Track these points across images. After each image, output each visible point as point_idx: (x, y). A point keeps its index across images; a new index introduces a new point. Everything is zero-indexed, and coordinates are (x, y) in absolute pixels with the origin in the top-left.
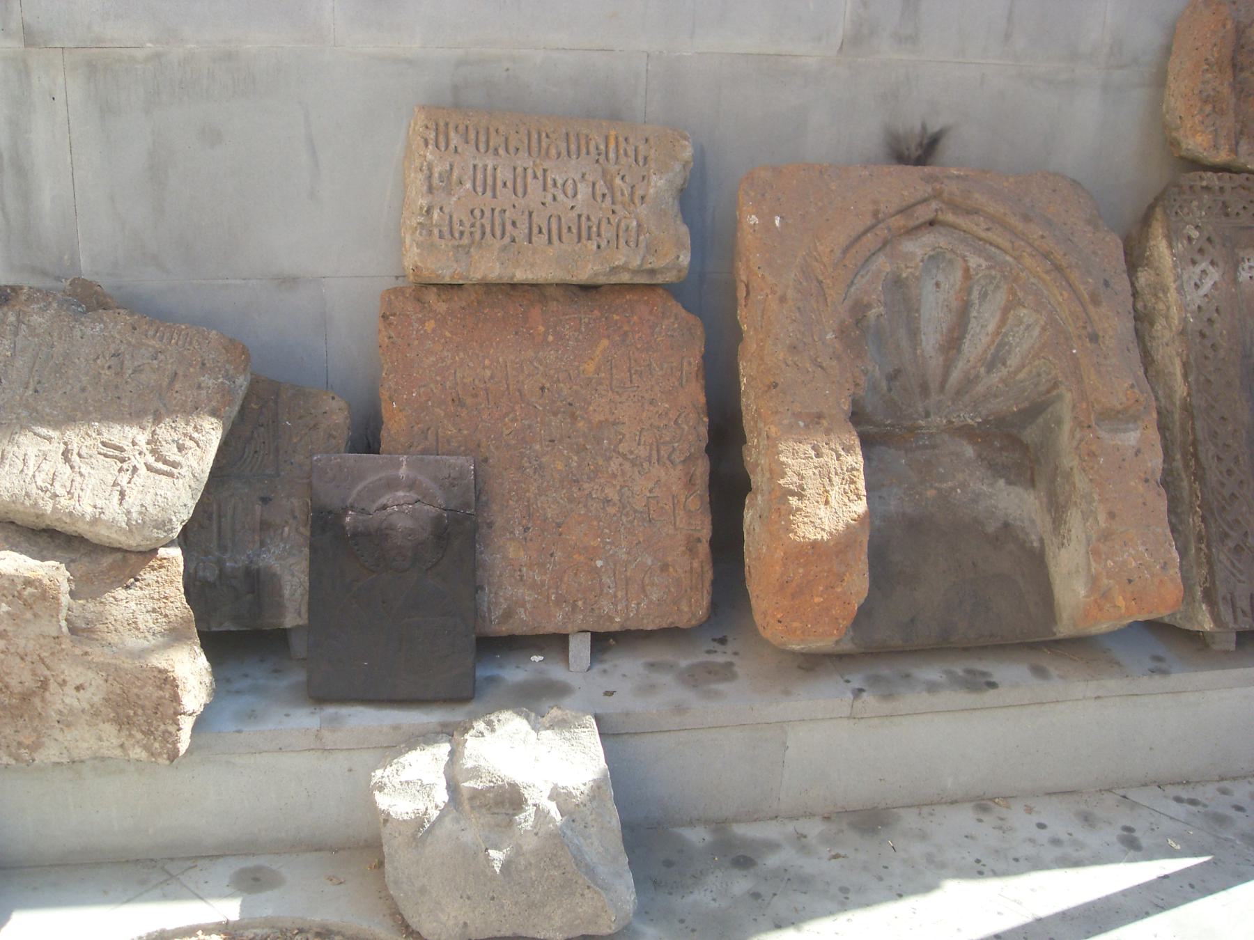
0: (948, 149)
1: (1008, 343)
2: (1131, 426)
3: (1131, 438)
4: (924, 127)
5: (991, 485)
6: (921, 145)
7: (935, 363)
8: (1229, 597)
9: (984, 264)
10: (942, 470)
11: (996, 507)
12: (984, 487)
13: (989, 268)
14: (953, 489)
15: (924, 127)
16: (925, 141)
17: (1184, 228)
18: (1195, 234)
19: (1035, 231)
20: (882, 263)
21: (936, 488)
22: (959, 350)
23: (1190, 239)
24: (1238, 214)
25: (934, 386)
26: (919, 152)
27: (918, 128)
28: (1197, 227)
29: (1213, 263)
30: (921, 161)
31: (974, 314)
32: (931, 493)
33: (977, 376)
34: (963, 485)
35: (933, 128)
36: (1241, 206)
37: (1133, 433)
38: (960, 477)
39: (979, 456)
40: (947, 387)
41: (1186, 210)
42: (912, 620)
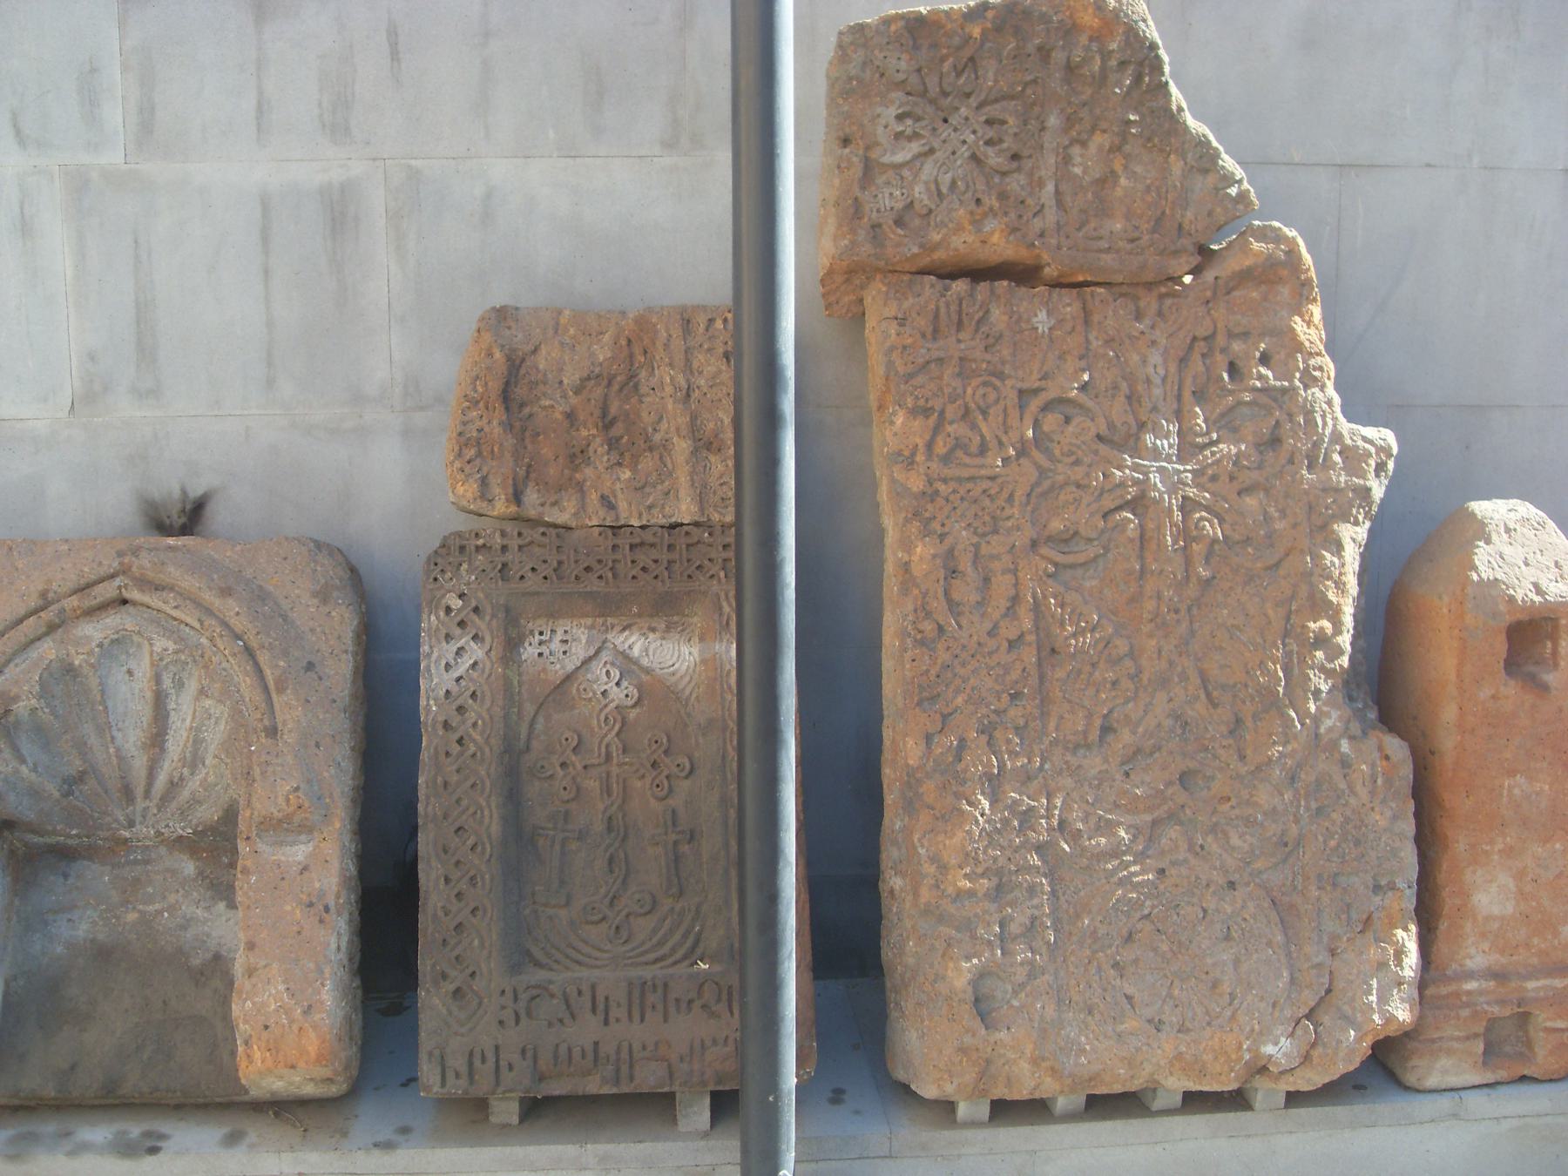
0: (218, 516)
1: (204, 740)
2: (303, 837)
3: (299, 852)
4: (184, 492)
5: (208, 908)
6: (183, 511)
7: (139, 763)
8: (437, 1052)
9: (171, 646)
10: (150, 890)
11: (208, 936)
12: (199, 912)
13: (176, 652)
14: (160, 912)
15: (184, 492)
16: (188, 507)
17: (444, 596)
18: (456, 603)
19: (231, 608)
20: (48, 650)
21: (140, 911)
22: (163, 750)
23: (448, 610)
24: (522, 577)
25: (139, 791)
26: (183, 520)
27: (177, 493)
28: (461, 596)
29: (475, 638)
30: (186, 530)
31: (172, 705)
32: (132, 917)
33: (181, 779)
34: (172, 909)
35: (196, 491)
36: (528, 567)
37: (303, 847)
38: (172, 898)
39: (200, 873)
40: (153, 791)
41: (449, 575)
42: (73, 1068)
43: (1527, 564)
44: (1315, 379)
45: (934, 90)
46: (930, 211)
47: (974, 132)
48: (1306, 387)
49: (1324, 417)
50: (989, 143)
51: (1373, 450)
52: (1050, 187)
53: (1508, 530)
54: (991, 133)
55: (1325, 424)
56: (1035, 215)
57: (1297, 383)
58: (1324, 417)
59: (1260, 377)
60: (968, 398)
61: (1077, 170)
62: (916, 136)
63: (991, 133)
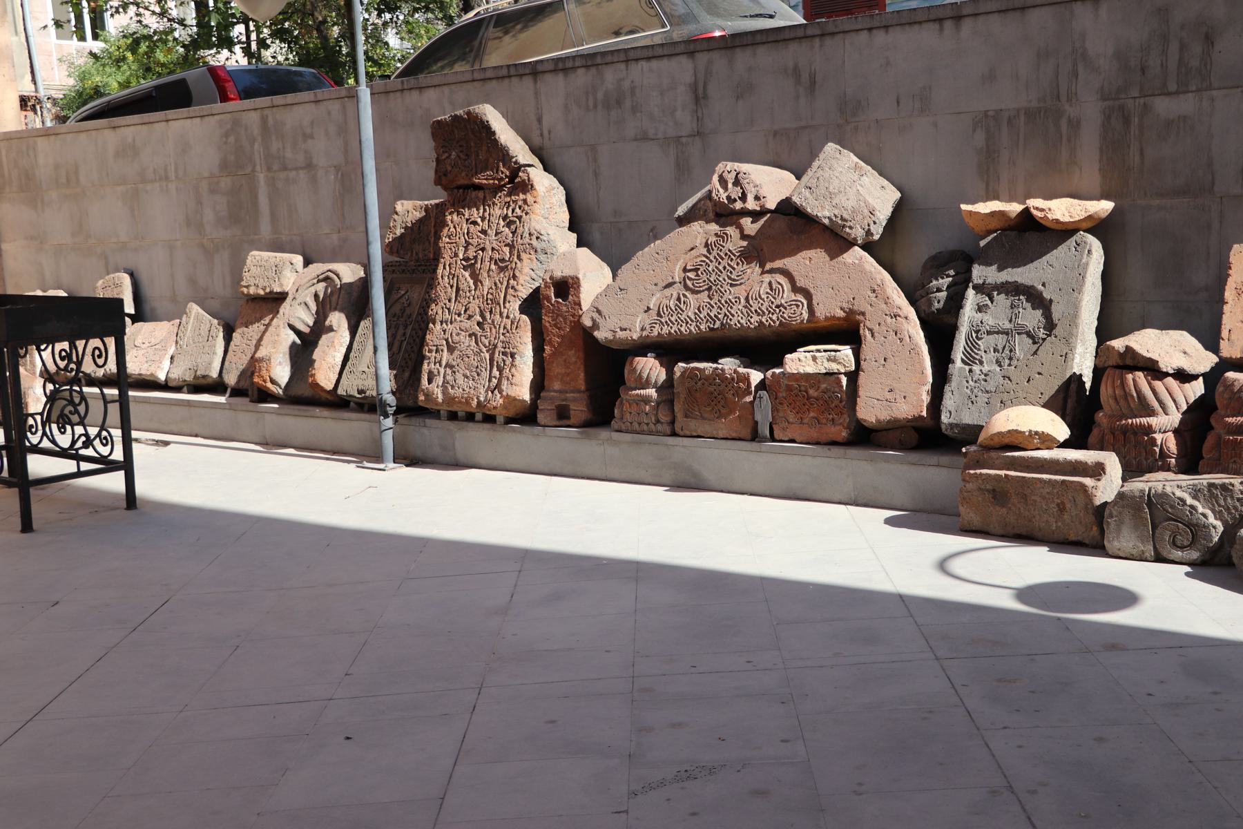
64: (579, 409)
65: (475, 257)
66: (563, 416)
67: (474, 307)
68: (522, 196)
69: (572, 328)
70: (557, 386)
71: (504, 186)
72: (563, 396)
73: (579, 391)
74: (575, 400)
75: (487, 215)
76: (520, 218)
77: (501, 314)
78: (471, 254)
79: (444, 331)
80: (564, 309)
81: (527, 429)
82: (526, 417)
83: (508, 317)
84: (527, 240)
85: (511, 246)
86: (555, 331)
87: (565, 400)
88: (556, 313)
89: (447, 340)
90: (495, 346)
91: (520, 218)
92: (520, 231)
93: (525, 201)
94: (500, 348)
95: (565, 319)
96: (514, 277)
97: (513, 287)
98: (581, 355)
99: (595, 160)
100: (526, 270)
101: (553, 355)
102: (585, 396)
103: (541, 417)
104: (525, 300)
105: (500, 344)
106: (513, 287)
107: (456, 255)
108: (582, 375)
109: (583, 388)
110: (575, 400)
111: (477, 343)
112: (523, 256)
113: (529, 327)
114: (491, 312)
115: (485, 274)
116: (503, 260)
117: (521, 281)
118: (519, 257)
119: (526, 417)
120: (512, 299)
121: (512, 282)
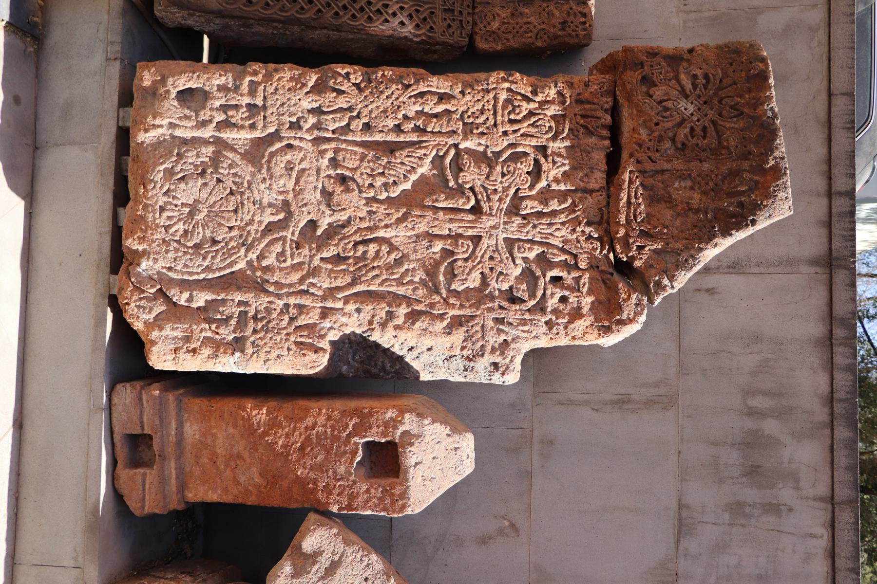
43: (434, 458)
44: (550, 329)
45: (722, 94)
46: (651, 96)
47: (698, 120)
48: (546, 323)
49: (528, 332)
50: (692, 129)
51: (507, 361)
52: (667, 166)
53: (456, 449)
54: (698, 130)
55: (524, 331)
56: (650, 158)
57: (549, 317)
58: (528, 332)
59: (552, 294)
60: (542, 117)
61: (677, 185)
62: (695, 86)
63: (698, 130)
64: (150, 495)
65: (460, 191)
66: (134, 449)
67: (353, 205)
68: (587, 302)
69: (301, 482)
70: (192, 431)
71: (612, 249)
72: (170, 449)
73: (182, 487)
74: (163, 480)
75: (554, 205)
76: (541, 308)
77: (331, 293)
78: (472, 176)
79: (295, 126)
80: (342, 470)
81: (101, 362)
82: (128, 354)
83: (325, 313)
84: (494, 339)
85: (480, 295)
86: (297, 440)
87: (163, 457)
88: (331, 445)
89: (275, 136)
90: (260, 288)
91: (541, 308)
92: (513, 314)
93: (576, 314)
94: (258, 303)
95: (320, 468)
96: (413, 316)
97: (390, 315)
98: (252, 500)
99: (650, 403)
100: (427, 342)
101: (249, 430)
102: (175, 504)
103: (126, 393)
104: (365, 339)
105: (264, 300)
106: (390, 315)
107: (469, 130)
108: (213, 497)
109: (192, 496)
110: (163, 480)
111: (270, 228)
112: (458, 336)
113: (304, 372)
114: (338, 259)
115: (422, 227)
116: (451, 275)
117: (403, 335)
118: (458, 322)
119: (128, 354)
120: (365, 316)
121: (403, 310)
